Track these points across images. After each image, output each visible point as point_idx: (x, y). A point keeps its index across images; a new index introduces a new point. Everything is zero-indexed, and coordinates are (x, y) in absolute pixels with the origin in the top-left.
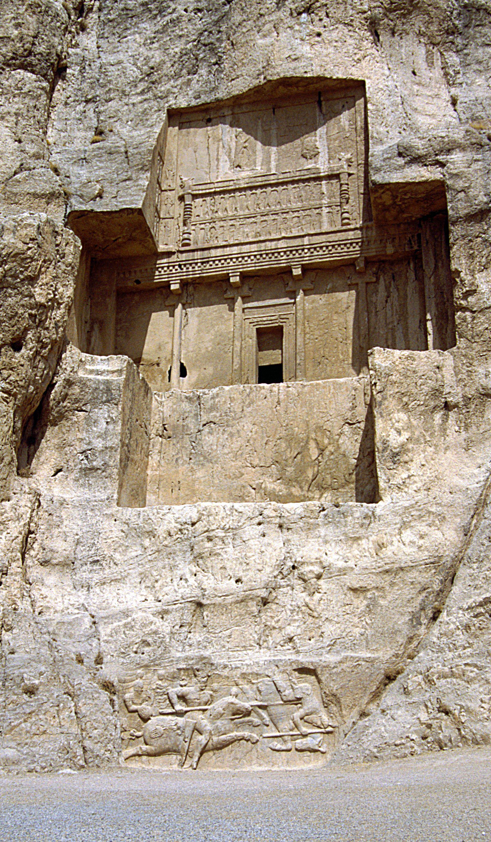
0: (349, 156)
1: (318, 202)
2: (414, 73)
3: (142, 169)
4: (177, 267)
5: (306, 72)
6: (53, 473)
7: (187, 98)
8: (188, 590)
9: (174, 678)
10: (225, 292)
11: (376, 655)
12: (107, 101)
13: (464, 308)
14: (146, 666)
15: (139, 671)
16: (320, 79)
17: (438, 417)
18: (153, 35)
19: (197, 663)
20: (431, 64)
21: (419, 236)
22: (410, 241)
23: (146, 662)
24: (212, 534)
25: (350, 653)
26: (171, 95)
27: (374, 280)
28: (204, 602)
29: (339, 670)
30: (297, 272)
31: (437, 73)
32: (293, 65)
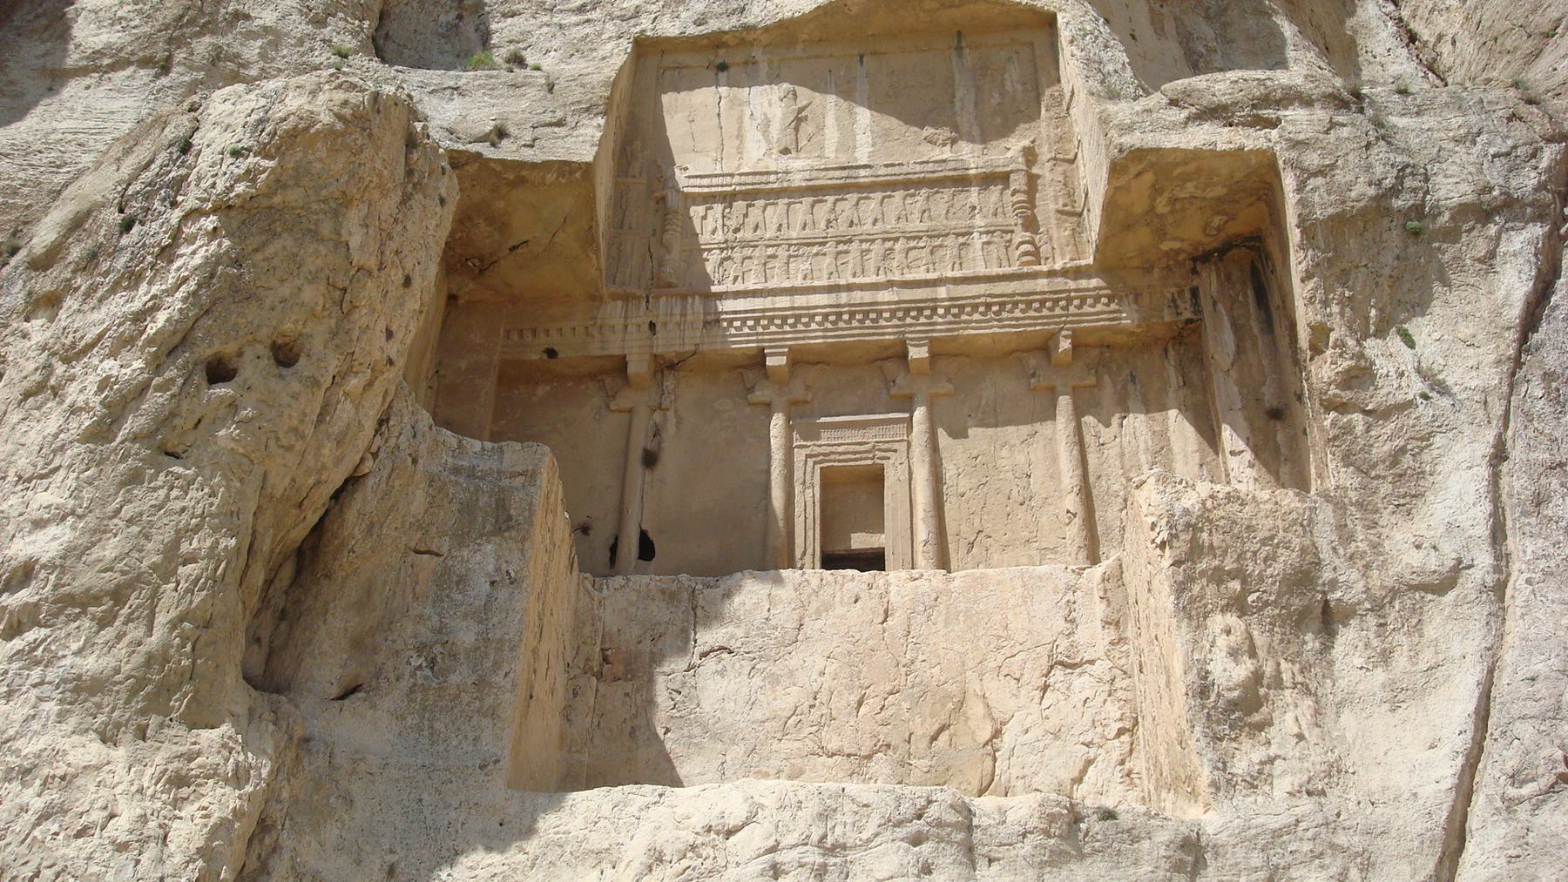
0: (1026, 143)
1: (964, 224)
2: (1133, 37)
3: (587, 110)
6: (335, 691)
7: (677, 23)
10: (751, 390)
12: (505, 15)
13: (1344, 404)
20: (1160, 32)
21: (1195, 293)
22: (1174, 300)
27: (1091, 380)
31: (1174, 49)
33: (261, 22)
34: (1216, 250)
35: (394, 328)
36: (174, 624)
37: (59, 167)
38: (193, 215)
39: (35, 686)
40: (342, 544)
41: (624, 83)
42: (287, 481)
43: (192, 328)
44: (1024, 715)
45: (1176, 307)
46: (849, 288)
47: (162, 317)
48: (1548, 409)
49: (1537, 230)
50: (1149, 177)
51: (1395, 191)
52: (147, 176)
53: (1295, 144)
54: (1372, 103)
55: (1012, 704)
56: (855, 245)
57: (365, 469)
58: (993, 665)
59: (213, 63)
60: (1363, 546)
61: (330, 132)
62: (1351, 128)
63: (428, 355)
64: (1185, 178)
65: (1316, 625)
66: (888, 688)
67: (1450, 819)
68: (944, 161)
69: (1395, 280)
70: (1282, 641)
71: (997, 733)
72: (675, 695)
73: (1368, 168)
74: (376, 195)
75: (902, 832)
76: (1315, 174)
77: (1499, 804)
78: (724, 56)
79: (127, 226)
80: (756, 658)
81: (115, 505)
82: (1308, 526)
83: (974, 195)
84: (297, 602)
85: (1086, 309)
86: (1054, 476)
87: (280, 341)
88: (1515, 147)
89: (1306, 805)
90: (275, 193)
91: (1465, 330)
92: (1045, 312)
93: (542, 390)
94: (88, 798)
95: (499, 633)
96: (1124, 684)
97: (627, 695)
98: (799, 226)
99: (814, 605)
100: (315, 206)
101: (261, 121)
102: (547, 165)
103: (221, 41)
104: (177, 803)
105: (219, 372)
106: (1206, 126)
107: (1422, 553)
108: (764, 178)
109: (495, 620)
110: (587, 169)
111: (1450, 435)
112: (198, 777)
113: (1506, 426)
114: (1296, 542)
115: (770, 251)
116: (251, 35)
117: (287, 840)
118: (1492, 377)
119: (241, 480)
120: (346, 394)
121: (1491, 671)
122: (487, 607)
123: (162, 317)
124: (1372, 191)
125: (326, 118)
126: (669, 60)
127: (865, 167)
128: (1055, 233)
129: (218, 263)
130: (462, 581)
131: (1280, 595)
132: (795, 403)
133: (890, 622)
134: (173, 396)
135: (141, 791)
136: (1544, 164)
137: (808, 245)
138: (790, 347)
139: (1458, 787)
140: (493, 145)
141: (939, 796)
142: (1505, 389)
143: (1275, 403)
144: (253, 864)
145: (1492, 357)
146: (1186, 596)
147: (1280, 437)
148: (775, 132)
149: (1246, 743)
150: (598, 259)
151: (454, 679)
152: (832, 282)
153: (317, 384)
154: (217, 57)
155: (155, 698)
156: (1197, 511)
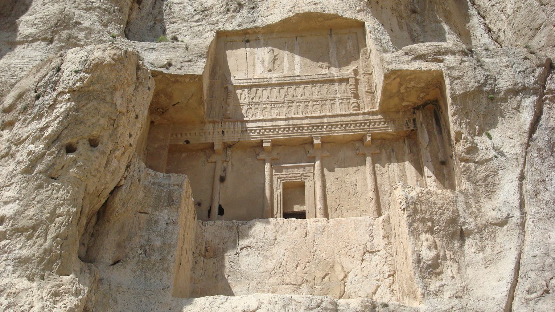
0: (355, 68)
2: (392, 30)
3: (200, 56)
5: (324, 11)
6: (111, 262)
7: (232, 25)
10: (258, 155)
12: (171, 23)
13: (467, 160)
16: (335, 17)
20: (401, 28)
21: (414, 120)
22: (407, 123)
27: (378, 151)
31: (406, 34)
32: (315, 6)
34: (421, 105)
35: (132, 133)
36: (54, 239)
37: (13, 76)
38: (61, 93)
39: (4, 260)
40: (114, 210)
41: (213, 46)
42: (94, 187)
43: (61, 133)
44: (355, 271)
45: (408, 125)
46: (293, 119)
47: (50, 130)
48: (539, 161)
49: (535, 98)
50: (398, 80)
51: (484, 84)
52: (45, 80)
53: (449, 68)
54: (476, 53)
55: (351, 266)
56: (295, 104)
57: (122, 183)
58: (344, 252)
59: (68, 40)
60: (474, 210)
61: (110, 64)
62: (469, 62)
63: (144, 143)
64: (411, 80)
65: (458, 238)
66: (307, 261)
67: (506, 306)
68: (326, 74)
69: (485, 116)
70: (446, 243)
72: (231, 263)
73: (475, 76)
74: (126, 86)
76: (456, 79)
77: (523, 301)
78: (248, 37)
79: (38, 98)
80: (260, 250)
81: (33, 196)
82: (455, 202)
83: (336, 86)
85: (376, 126)
86: (365, 185)
87: (92, 138)
88: (526, 69)
89: (455, 301)
90: (90, 86)
91: (510, 133)
92: (362, 127)
93: (184, 155)
95: (169, 241)
96: (391, 259)
97: (214, 263)
98: (275, 97)
99: (281, 231)
100: (104, 91)
101: (85, 61)
102: (186, 76)
103: (71, 32)
104: (55, 302)
105: (70, 149)
106: (418, 62)
107: (495, 212)
108: (262, 80)
109: (168, 237)
110: (200, 77)
111: (505, 170)
112: (62, 293)
113: (524, 167)
114: (451, 208)
115: (265, 106)
116: (81, 30)
118: (519, 150)
119: (78, 188)
120: (115, 157)
121: (520, 254)
122: (165, 232)
124: (476, 85)
125: (108, 60)
126: (229, 39)
127: (298, 76)
128: (365, 99)
129: (70, 111)
130: (156, 223)
131: (445, 227)
132: (273, 159)
133: (308, 237)
134: (54, 158)
135: (42, 298)
136: (537, 75)
137: (278, 104)
138: (272, 140)
139: (509, 295)
140: (167, 68)
141: (326, 299)
142: (524, 154)
143: (443, 159)
145: (519, 143)
146: (412, 228)
147: (445, 171)
148: (266, 64)
149: (434, 280)
150: (204, 109)
151: (153, 258)
152: (287, 117)
153: (105, 153)
154: (69, 37)
155: (47, 265)
156: (416, 197)
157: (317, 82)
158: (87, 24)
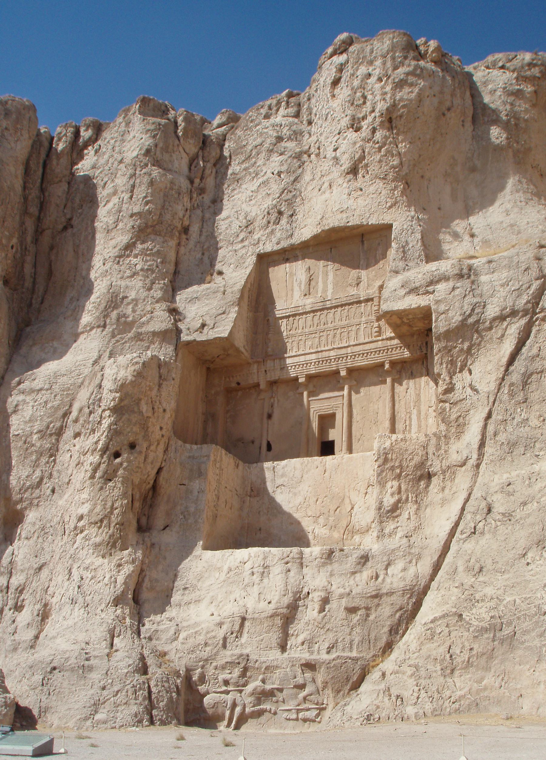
1: (359, 320)
3: (233, 304)
4: (264, 372)
6: (162, 528)
8: (237, 609)
9: (223, 668)
11: (361, 655)
14: (206, 660)
15: (201, 663)
17: (422, 483)
18: (251, 194)
19: (238, 658)
23: (206, 657)
24: (255, 570)
25: (342, 654)
26: (261, 242)
28: (247, 616)
29: (332, 665)
30: (343, 373)
33: (130, 298)
35: (162, 426)
41: (253, 274)
46: (322, 351)
51: (470, 315)
53: (437, 302)
57: (163, 465)
61: (132, 381)
67: (445, 544)
71: (352, 508)
75: (283, 561)
78: (288, 255)
82: (425, 447)
84: (153, 502)
85: (394, 352)
86: (385, 413)
89: (405, 540)
93: (240, 393)
94: (100, 573)
105: (117, 455)
114: (420, 454)
116: (128, 304)
117: (148, 573)
118: (493, 386)
121: (470, 494)
122: (197, 500)
123: (101, 443)
124: (460, 318)
125: (130, 378)
131: (413, 471)
135: (111, 570)
142: (496, 391)
144: (140, 579)
145: (494, 378)
146: (380, 477)
151: (190, 521)
155: (113, 545)
157: (345, 305)
158: (132, 295)
